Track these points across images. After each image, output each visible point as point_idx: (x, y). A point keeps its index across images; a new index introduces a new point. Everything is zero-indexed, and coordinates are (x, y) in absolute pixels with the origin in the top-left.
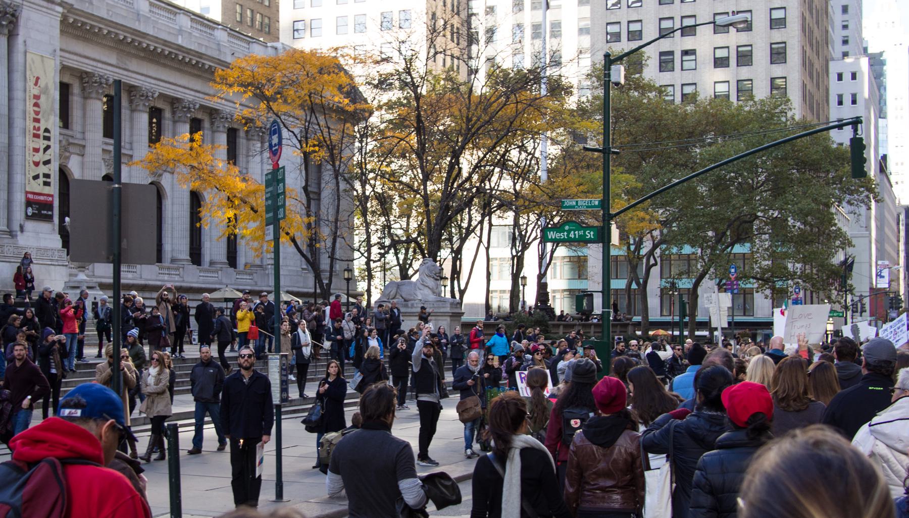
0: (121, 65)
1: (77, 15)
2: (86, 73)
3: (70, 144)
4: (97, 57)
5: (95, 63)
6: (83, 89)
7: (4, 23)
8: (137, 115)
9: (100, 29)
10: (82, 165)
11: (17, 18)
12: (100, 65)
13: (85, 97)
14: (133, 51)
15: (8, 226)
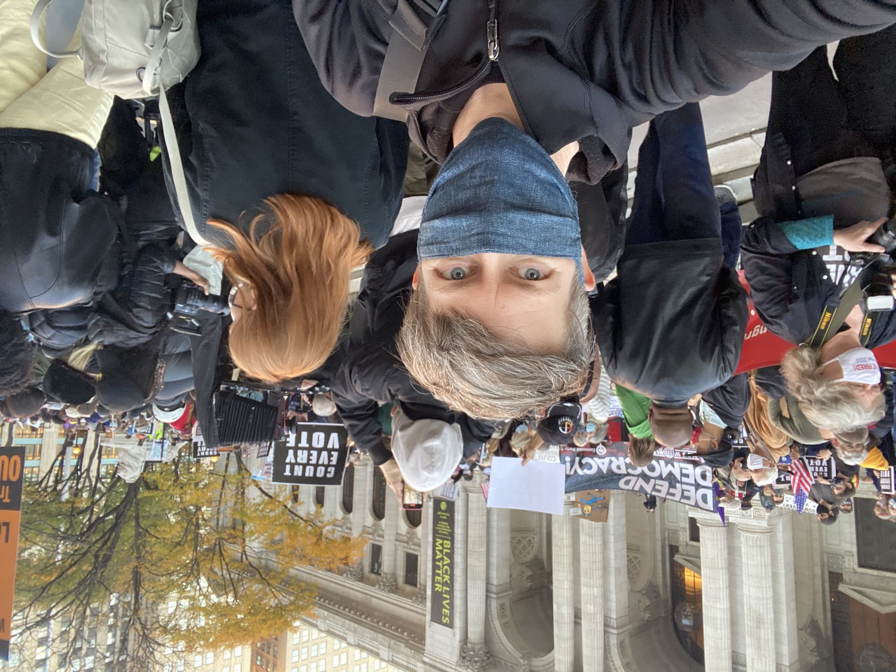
0: (368, 597)
1: (401, 638)
2: (393, 592)
3: (407, 543)
4: (386, 604)
5: (387, 599)
6: (395, 580)
7: (472, 653)
8: (359, 561)
9: (384, 626)
10: (397, 527)
11: (461, 655)
12: (384, 598)
13: (394, 576)
14: (360, 607)
15: (468, 496)
